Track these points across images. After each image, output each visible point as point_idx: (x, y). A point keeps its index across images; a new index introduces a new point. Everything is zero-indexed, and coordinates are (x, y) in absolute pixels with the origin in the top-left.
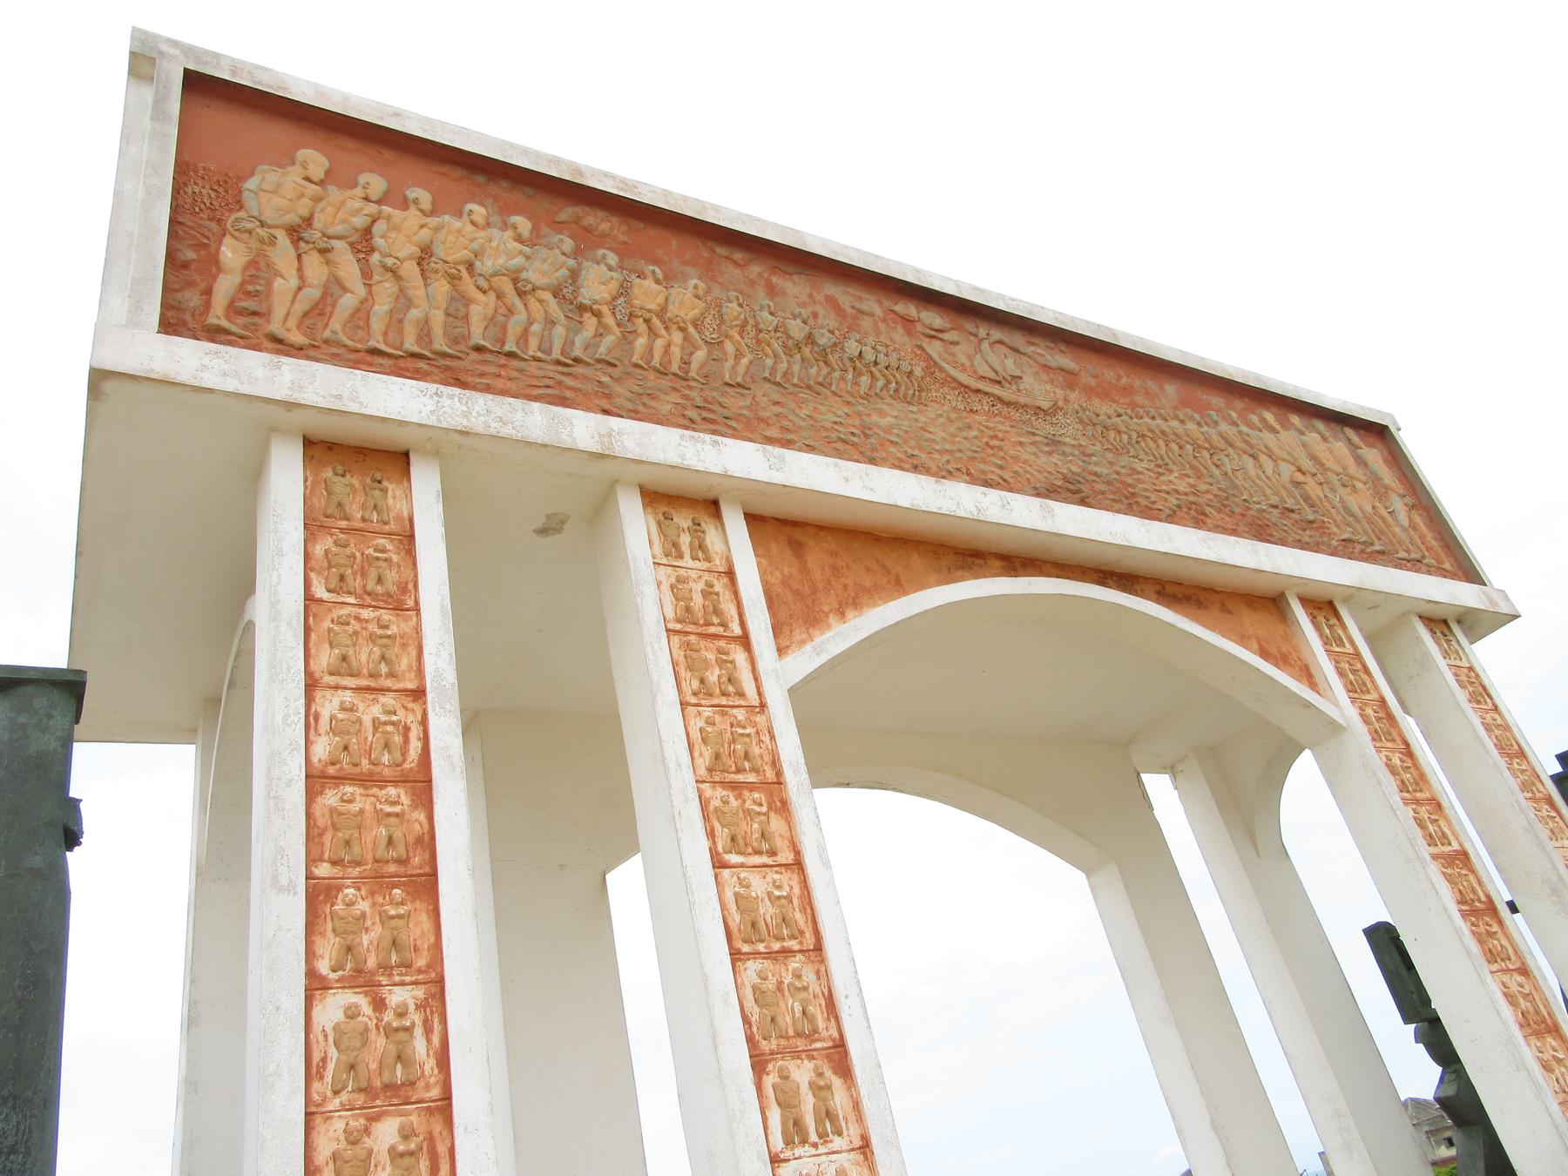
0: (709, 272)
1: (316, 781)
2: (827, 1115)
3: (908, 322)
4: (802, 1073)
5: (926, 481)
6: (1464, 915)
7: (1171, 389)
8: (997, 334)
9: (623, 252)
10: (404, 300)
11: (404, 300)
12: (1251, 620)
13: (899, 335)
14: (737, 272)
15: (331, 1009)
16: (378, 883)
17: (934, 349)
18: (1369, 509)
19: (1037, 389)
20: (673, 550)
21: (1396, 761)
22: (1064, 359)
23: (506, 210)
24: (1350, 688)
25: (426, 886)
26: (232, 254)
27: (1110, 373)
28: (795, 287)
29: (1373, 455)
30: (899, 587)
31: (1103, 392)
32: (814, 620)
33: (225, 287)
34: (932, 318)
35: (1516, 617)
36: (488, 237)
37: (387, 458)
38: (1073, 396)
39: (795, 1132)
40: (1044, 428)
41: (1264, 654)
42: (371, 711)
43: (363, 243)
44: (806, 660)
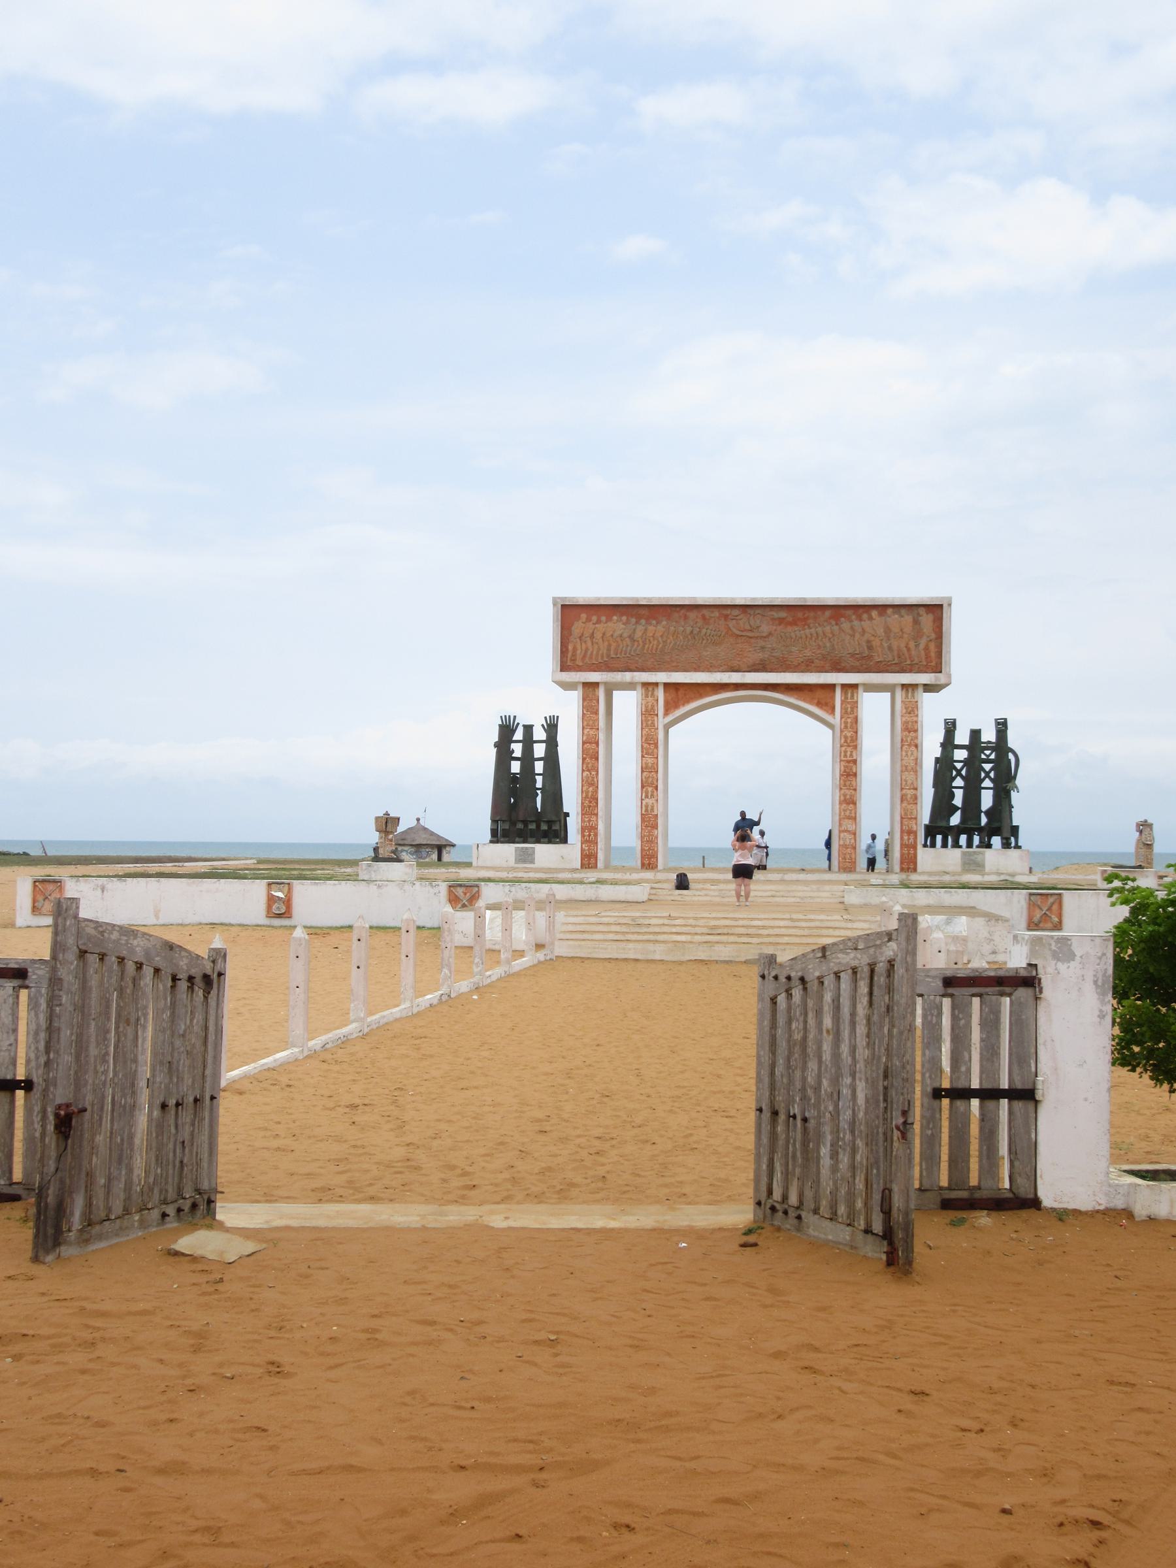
0: (669, 618)
1: (584, 743)
2: (652, 796)
3: (726, 617)
4: (650, 789)
5: (708, 674)
6: (841, 775)
7: (828, 613)
8: (758, 611)
9: (647, 619)
10: (599, 649)
11: (599, 649)
12: (819, 694)
13: (722, 622)
14: (676, 615)
15: (586, 773)
16: (591, 758)
17: (731, 624)
18: (903, 645)
19: (765, 628)
20: (647, 696)
21: (849, 734)
22: (783, 614)
23: (622, 615)
24: (844, 713)
25: (597, 759)
26: (570, 648)
27: (800, 615)
28: (692, 615)
29: (927, 620)
30: (701, 696)
31: (794, 623)
32: (676, 707)
33: (570, 655)
34: (736, 612)
35: (947, 685)
36: (617, 626)
37: (596, 685)
38: (779, 628)
39: (647, 797)
40: (761, 643)
41: (819, 704)
42: (592, 732)
43: (592, 636)
44: (670, 718)
